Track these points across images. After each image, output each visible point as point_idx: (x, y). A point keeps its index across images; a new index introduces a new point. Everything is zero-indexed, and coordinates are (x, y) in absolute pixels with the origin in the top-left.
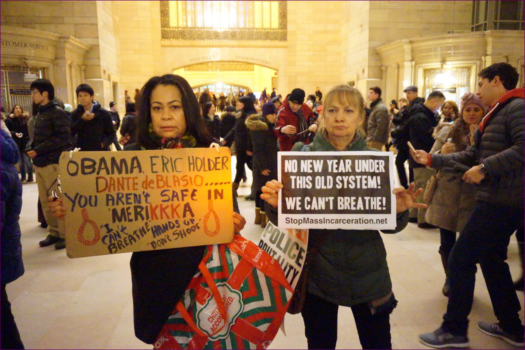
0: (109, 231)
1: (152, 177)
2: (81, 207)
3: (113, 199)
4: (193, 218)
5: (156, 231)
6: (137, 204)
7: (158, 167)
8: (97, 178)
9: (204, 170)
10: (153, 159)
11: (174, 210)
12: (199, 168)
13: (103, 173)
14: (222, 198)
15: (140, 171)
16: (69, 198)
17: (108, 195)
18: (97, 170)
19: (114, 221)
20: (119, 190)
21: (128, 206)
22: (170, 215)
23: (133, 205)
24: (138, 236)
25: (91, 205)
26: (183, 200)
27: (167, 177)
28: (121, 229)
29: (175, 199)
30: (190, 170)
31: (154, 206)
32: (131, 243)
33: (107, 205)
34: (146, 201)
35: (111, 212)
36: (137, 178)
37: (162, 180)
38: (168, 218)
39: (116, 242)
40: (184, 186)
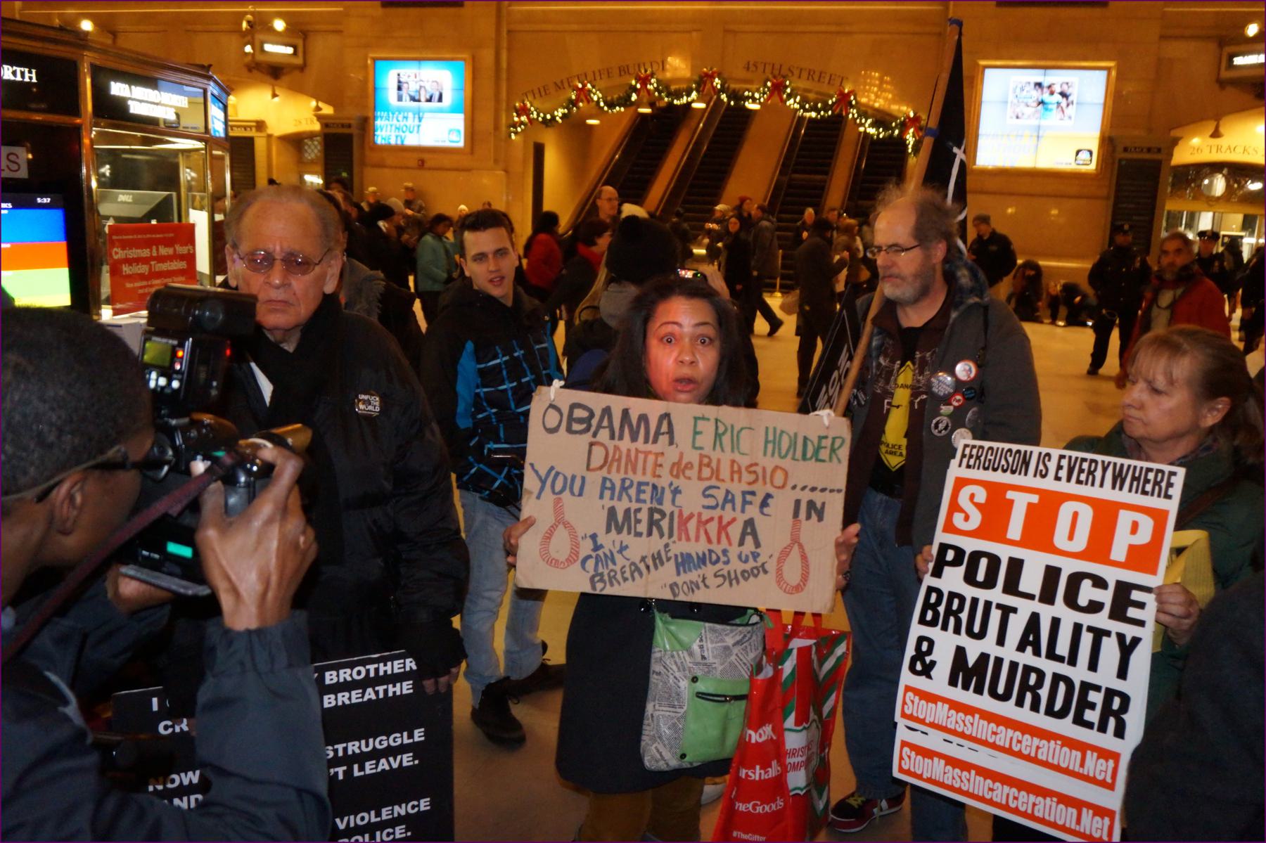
0: (597, 547)
1: (692, 457)
2: (554, 492)
3: (613, 489)
4: (758, 550)
5: (683, 563)
6: (655, 505)
7: (706, 440)
8: (591, 444)
9: (793, 459)
10: (700, 423)
11: (723, 528)
12: (783, 453)
13: (604, 435)
14: (820, 519)
15: (671, 442)
16: (536, 472)
17: (605, 479)
18: (593, 429)
19: (608, 530)
20: (626, 472)
24: (648, 567)
25: (572, 493)
26: (743, 511)
27: (719, 461)
28: (618, 548)
29: (729, 506)
30: (765, 454)
31: (686, 514)
32: (633, 579)
33: (601, 497)
35: (604, 515)
36: (663, 454)
37: (708, 465)
38: (709, 541)
39: (606, 572)
40: (750, 484)
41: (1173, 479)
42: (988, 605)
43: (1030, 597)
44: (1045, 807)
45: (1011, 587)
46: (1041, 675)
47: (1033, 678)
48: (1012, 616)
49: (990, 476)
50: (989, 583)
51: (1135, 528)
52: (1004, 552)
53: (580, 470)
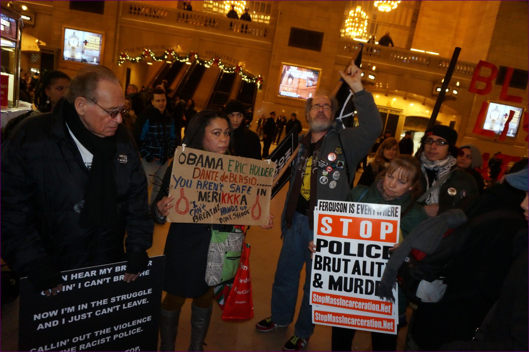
3: (201, 185)
6: (215, 191)
11: (236, 199)
14: (265, 195)
17: (199, 181)
21: (209, 191)
22: (233, 201)
23: (213, 191)
29: (238, 191)
31: (224, 194)
33: (197, 188)
34: (221, 190)
41: (397, 210)
42: (339, 260)
43: (355, 255)
44: (370, 323)
45: (347, 253)
46: (361, 281)
47: (359, 283)
48: (349, 262)
49: (335, 213)
50: (339, 252)
51: (387, 228)
52: (343, 241)
53: (191, 178)
